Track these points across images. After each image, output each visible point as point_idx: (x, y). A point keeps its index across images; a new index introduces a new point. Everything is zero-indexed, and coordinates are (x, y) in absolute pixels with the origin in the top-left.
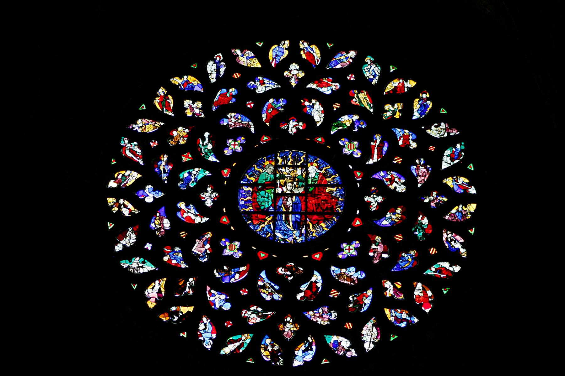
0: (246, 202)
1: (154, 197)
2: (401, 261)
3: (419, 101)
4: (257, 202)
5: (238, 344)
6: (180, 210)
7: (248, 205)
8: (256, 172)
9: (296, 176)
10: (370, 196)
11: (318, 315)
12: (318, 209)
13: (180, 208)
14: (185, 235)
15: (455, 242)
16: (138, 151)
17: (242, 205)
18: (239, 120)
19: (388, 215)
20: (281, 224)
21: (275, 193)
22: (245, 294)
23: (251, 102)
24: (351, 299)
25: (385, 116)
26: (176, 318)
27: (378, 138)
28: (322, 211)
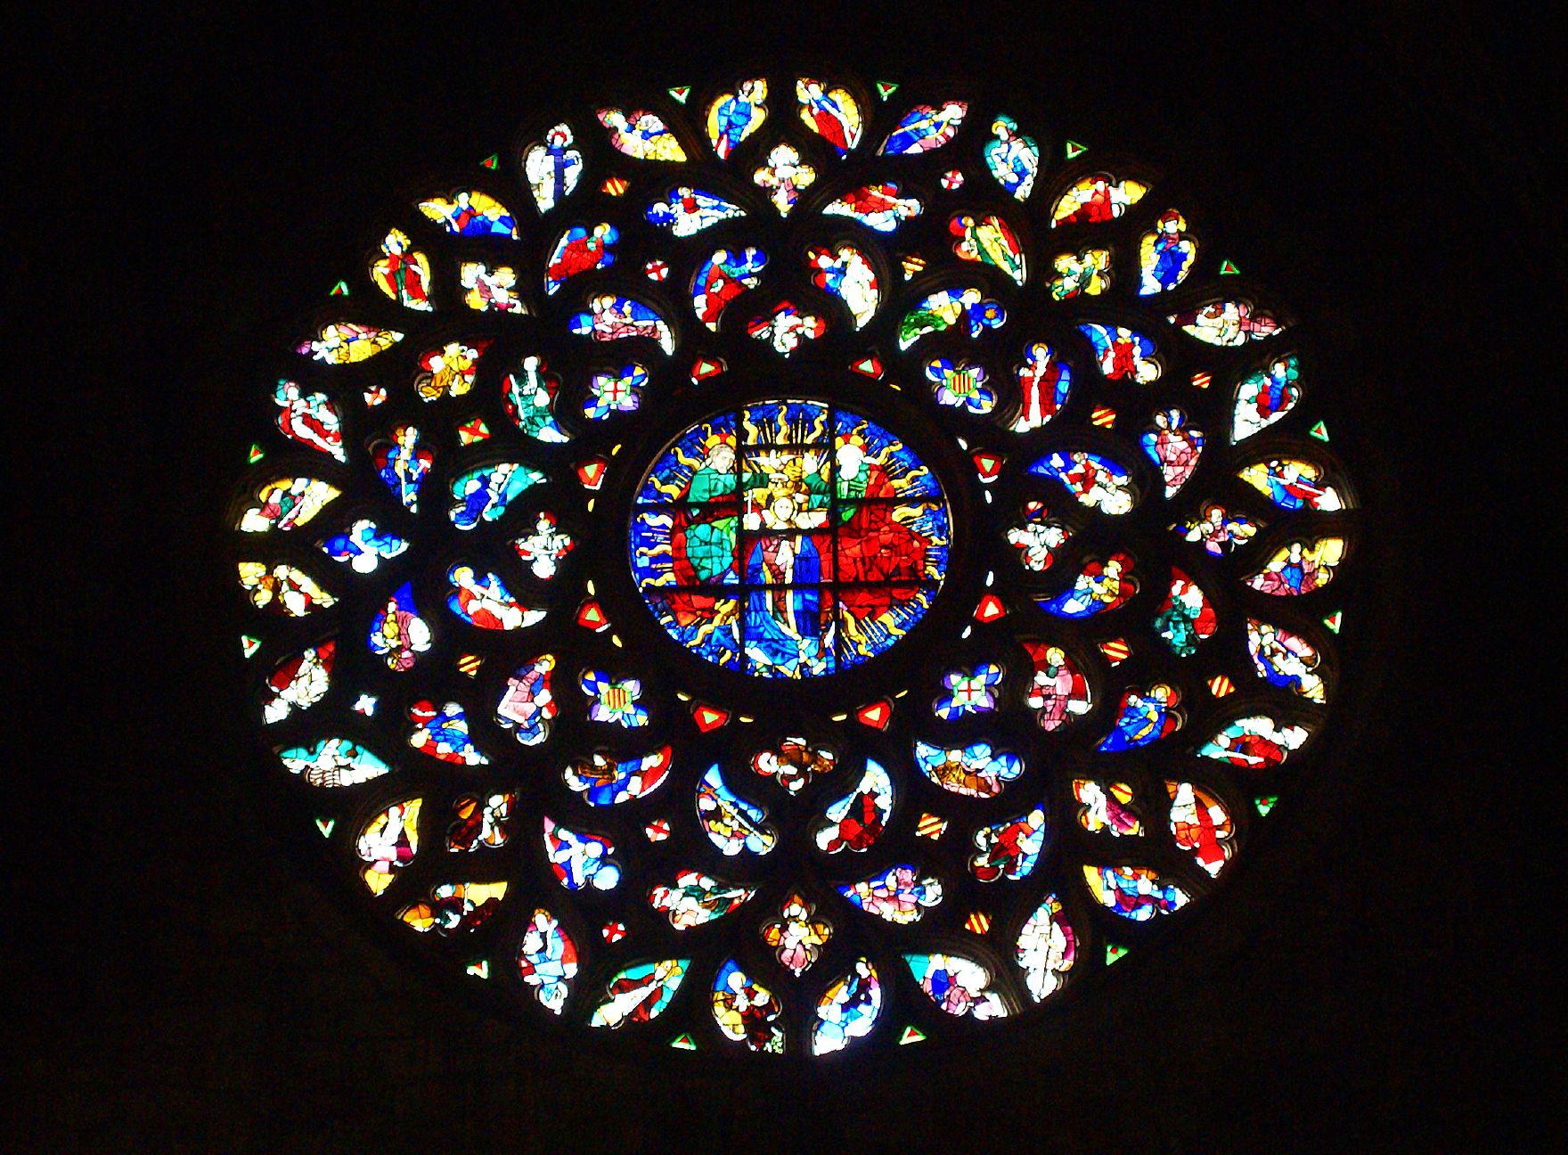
0: (654, 560)
1: (379, 555)
2: (1127, 720)
3: (1156, 244)
4: (688, 558)
5: (642, 993)
6: (458, 591)
7: (659, 568)
8: (681, 468)
9: (801, 477)
10: (1023, 527)
11: (883, 893)
12: (870, 573)
13: (457, 585)
14: (473, 665)
15: (1285, 656)
16: (331, 422)
17: (644, 568)
18: (626, 317)
19: (1083, 582)
20: (761, 622)
21: (740, 529)
22: (662, 837)
23: (659, 263)
24: (981, 840)
25: (1060, 289)
26: (454, 921)
27: (1041, 354)
28: (882, 579)
